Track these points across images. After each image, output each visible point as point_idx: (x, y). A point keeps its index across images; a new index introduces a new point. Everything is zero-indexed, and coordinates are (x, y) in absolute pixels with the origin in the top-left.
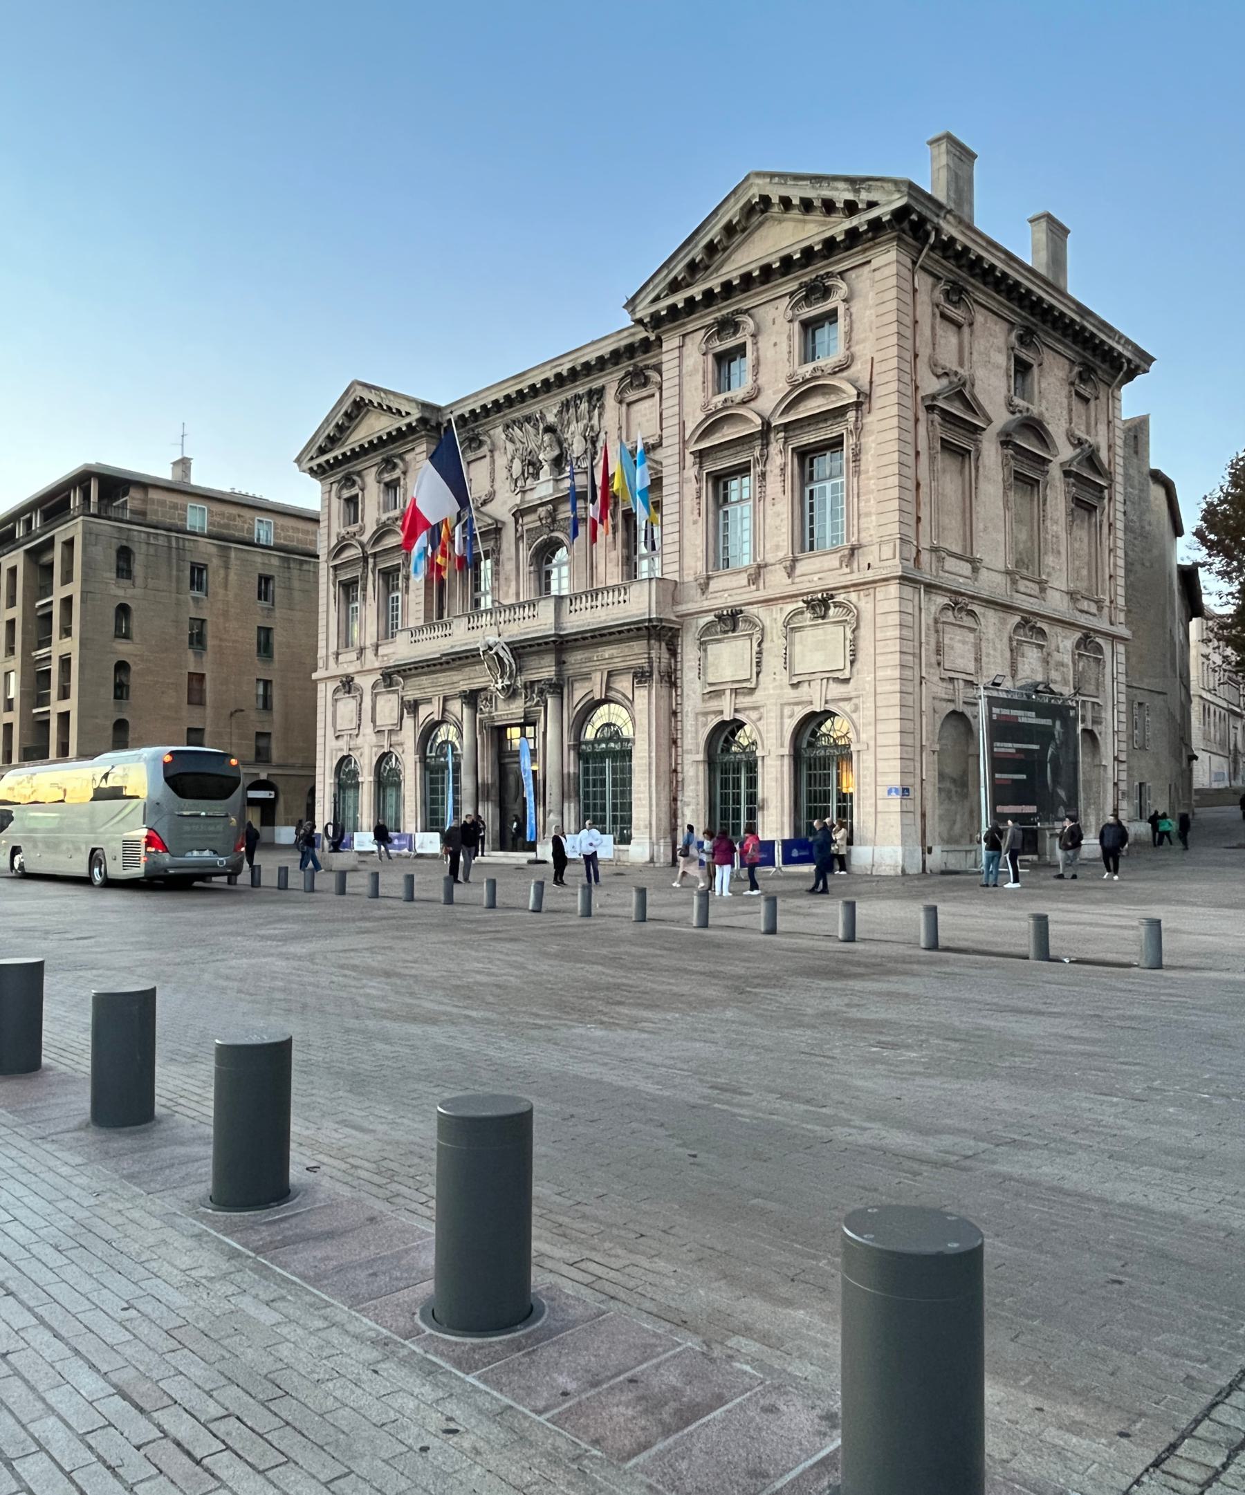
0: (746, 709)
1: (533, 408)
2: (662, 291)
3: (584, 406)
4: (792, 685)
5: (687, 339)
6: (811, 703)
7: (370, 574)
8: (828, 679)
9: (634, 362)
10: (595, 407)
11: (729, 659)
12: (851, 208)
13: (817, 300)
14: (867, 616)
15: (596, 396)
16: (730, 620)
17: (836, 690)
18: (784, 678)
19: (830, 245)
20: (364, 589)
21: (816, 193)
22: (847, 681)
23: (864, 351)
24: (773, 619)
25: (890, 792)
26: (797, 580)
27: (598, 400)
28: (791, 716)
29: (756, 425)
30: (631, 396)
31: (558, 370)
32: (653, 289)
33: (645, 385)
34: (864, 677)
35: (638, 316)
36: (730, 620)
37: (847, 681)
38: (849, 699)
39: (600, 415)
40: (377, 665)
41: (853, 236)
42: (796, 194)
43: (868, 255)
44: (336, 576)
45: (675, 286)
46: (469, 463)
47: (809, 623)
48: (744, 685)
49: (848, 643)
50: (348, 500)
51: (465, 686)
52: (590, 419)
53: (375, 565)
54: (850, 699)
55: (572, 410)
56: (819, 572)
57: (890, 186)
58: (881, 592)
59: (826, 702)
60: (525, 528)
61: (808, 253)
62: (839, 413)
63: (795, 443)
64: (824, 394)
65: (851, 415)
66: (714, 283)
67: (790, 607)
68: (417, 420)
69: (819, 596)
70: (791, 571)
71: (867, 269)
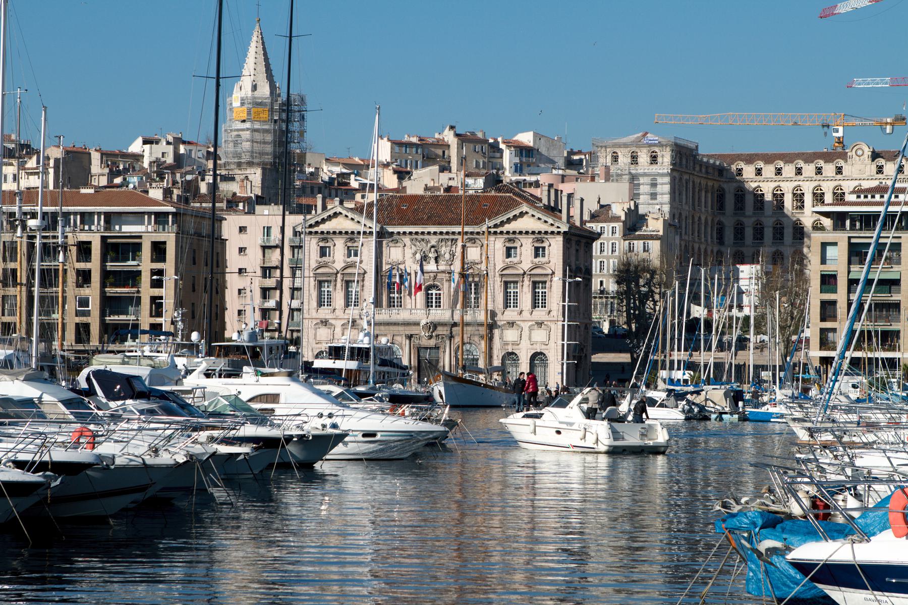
1: (426, 237)
11: (511, 335)
15: (454, 241)
16: (511, 324)
17: (544, 347)
18: (528, 342)
19: (546, 233)
23: (553, 261)
24: (526, 326)
29: (522, 272)
34: (552, 344)
36: (511, 324)
41: (552, 233)
50: (321, 247)
51: (409, 333)
55: (443, 243)
61: (540, 233)
62: (547, 275)
67: (531, 323)
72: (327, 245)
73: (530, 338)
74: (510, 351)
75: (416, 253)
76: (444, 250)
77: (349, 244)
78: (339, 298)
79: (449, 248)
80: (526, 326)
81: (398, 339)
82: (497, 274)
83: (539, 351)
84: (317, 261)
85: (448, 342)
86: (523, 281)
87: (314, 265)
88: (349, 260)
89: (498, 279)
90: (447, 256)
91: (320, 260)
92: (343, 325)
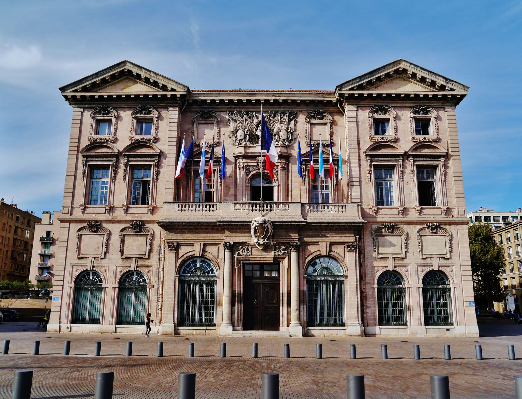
0: (399, 266)
2: (355, 87)
3: (286, 117)
4: (423, 259)
5: (359, 109)
6: (432, 266)
7: (122, 165)
8: (440, 257)
9: (320, 108)
10: (291, 120)
12: (442, 88)
13: (423, 114)
14: (455, 235)
17: (443, 262)
19: (435, 96)
20: (116, 173)
21: (429, 78)
22: (448, 259)
25: (470, 304)
26: (422, 216)
27: (294, 118)
28: (422, 271)
30: (313, 121)
31: (277, 98)
32: (352, 85)
33: (321, 119)
35: (343, 92)
37: (448, 259)
38: (449, 266)
39: (295, 125)
40: (129, 217)
42: (420, 74)
43: (444, 105)
44: (87, 161)
45: (361, 87)
46: (199, 124)
47: (428, 234)
48: (399, 256)
49: (447, 244)
52: (289, 124)
53: (128, 161)
54: (449, 266)
55: (277, 118)
56: (431, 215)
57: (462, 87)
58: (459, 227)
59: (439, 267)
60: (246, 164)
62: (438, 157)
63: (417, 163)
64: (428, 148)
65: (442, 158)
66: (374, 92)
68: (181, 95)
69: (435, 224)
70: (420, 213)
71: (442, 109)
72: (106, 117)
73: (421, 250)
74: (390, 268)
75: (237, 130)
76: (279, 127)
77: (140, 116)
78: (120, 190)
79: (284, 126)
80: (413, 230)
81: (212, 250)
82: (363, 156)
83: (435, 268)
84: (89, 139)
85: (294, 254)
86: (403, 166)
87: (85, 142)
88: (138, 137)
89: (366, 163)
90: (283, 134)
91: (95, 137)
92: (122, 230)
